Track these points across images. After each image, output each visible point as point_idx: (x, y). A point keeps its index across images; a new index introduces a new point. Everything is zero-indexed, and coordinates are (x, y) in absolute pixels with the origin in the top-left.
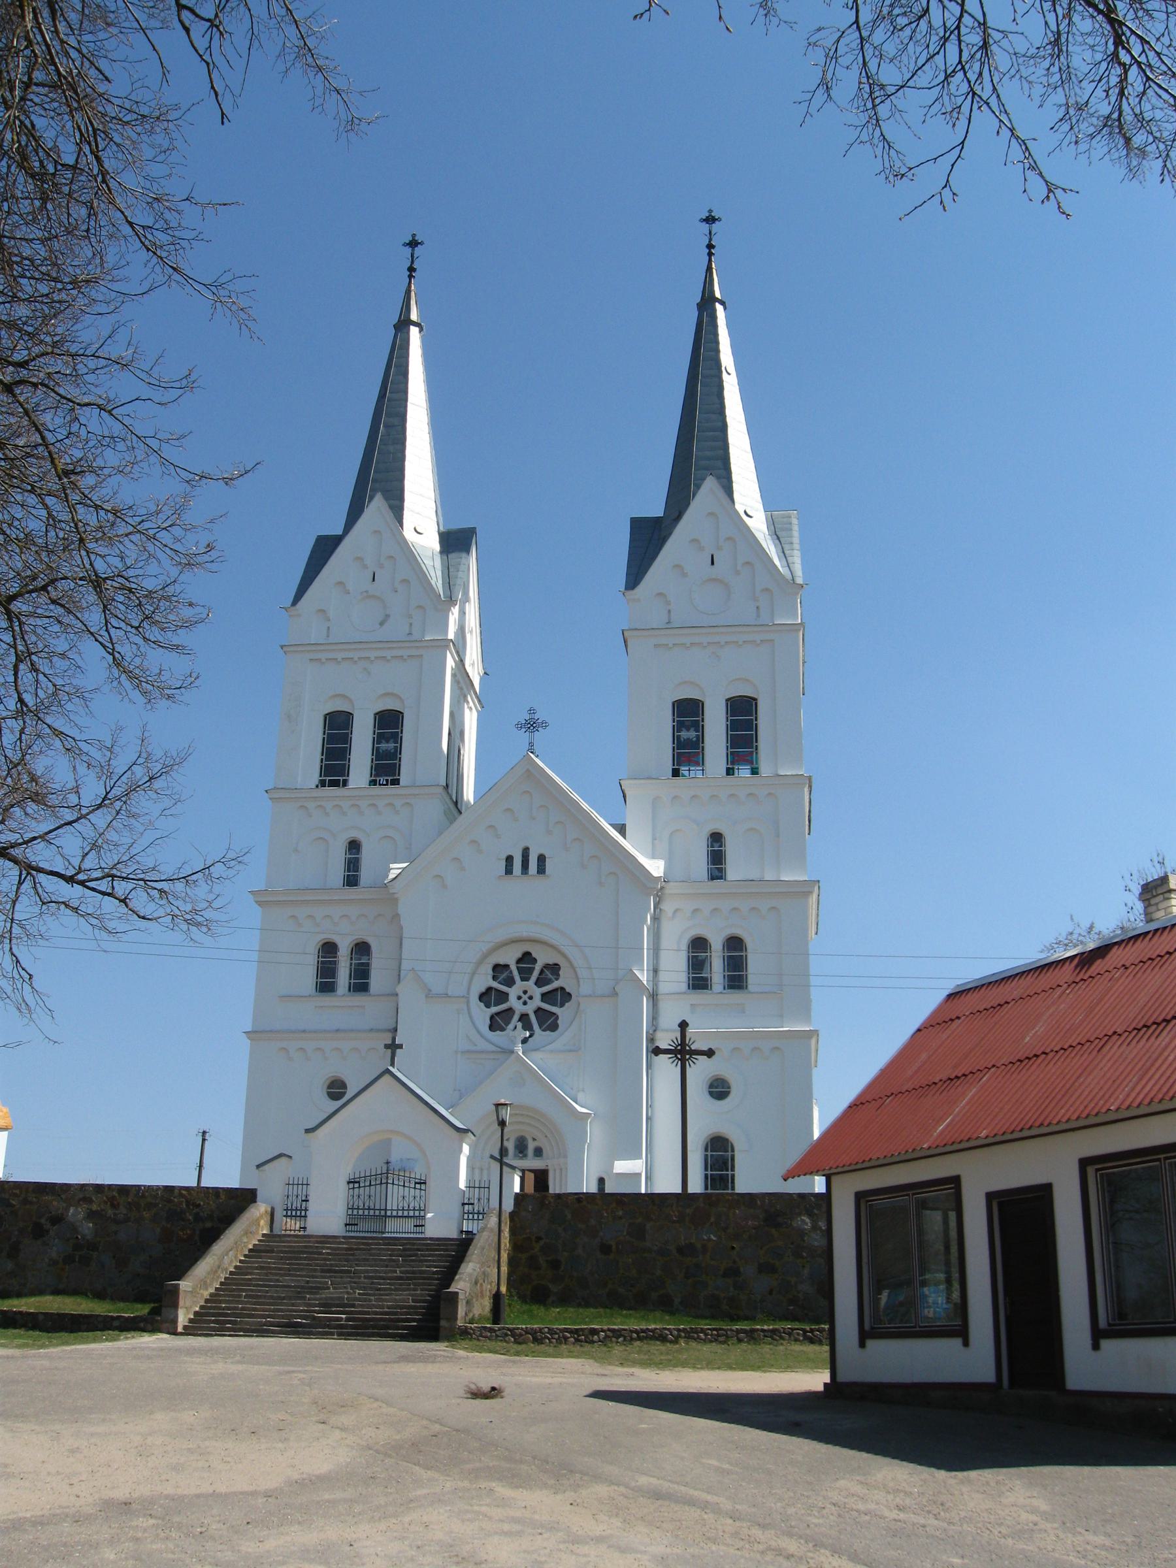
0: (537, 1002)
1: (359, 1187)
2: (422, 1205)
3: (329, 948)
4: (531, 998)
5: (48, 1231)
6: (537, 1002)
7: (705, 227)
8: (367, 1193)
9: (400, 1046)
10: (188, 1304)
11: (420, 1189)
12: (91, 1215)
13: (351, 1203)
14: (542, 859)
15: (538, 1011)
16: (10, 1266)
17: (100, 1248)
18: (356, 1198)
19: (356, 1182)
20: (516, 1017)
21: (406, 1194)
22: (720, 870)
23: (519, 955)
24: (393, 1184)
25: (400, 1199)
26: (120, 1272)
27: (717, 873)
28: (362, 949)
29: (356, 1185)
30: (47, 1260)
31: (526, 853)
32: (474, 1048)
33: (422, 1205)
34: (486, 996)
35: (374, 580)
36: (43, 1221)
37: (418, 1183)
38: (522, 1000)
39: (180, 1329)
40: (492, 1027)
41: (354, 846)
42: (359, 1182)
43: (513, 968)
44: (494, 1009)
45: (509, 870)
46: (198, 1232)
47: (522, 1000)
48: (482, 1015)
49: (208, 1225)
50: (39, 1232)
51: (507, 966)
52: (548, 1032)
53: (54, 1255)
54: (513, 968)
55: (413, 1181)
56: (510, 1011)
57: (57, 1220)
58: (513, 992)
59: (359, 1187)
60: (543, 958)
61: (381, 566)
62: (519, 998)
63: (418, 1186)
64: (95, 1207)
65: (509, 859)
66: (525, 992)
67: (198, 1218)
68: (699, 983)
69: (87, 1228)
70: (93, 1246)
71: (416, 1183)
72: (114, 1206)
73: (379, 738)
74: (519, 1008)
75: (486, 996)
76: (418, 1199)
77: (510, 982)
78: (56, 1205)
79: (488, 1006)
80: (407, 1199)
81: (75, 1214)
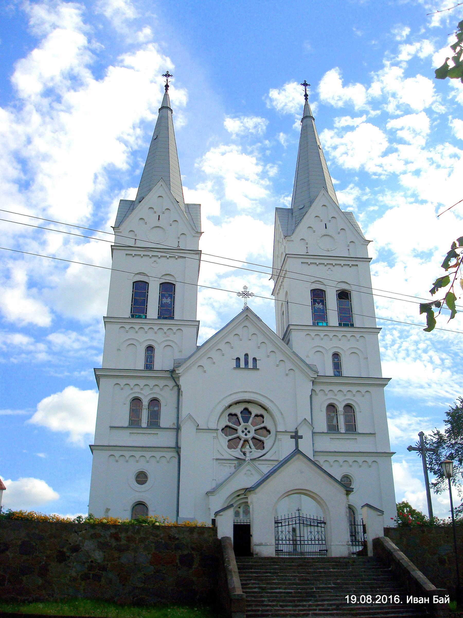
1: (282, 526)
2: (323, 537)
3: (136, 401)
4: (249, 432)
5: (68, 557)
6: (252, 434)
8: (287, 529)
9: (301, 437)
11: (321, 527)
12: (102, 546)
13: (277, 537)
14: (255, 360)
15: (254, 438)
16: (40, 581)
17: (108, 569)
18: (280, 533)
19: (279, 523)
21: (312, 530)
22: (339, 372)
23: (242, 409)
24: (303, 524)
25: (309, 533)
26: (123, 585)
27: (337, 373)
28: (155, 402)
29: (280, 525)
30: (68, 577)
31: (246, 355)
32: (222, 457)
33: (323, 537)
34: (227, 429)
35: (159, 219)
36: (65, 550)
37: (319, 523)
38: (244, 433)
40: (230, 447)
41: (150, 349)
42: (281, 523)
43: (239, 415)
44: (230, 437)
45: (238, 366)
46: (178, 557)
47: (244, 433)
48: (223, 440)
49: (185, 552)
51: (235, 415)
52: (259, 450)
53: (74, 574)
54: (239, 415)
55: (316, 521)
56: (239, 438)
57: (76, 549)
58: (240, 429)
59: (282, 526)
61: (163, 213)
62: (243, 432)
63: (319, 525)
65: (238, 359)
66: (246, 429)
67: (178, 547)
69: (98, 556)
70: (104, 568)
71: (318, 523)
72: (118, 539)
73: (162, 296)
75: (227, 429)
76: (320, 533)
78: (74, 538)
79: (226, 435)
80: (313, 533)
81: (88, 545)
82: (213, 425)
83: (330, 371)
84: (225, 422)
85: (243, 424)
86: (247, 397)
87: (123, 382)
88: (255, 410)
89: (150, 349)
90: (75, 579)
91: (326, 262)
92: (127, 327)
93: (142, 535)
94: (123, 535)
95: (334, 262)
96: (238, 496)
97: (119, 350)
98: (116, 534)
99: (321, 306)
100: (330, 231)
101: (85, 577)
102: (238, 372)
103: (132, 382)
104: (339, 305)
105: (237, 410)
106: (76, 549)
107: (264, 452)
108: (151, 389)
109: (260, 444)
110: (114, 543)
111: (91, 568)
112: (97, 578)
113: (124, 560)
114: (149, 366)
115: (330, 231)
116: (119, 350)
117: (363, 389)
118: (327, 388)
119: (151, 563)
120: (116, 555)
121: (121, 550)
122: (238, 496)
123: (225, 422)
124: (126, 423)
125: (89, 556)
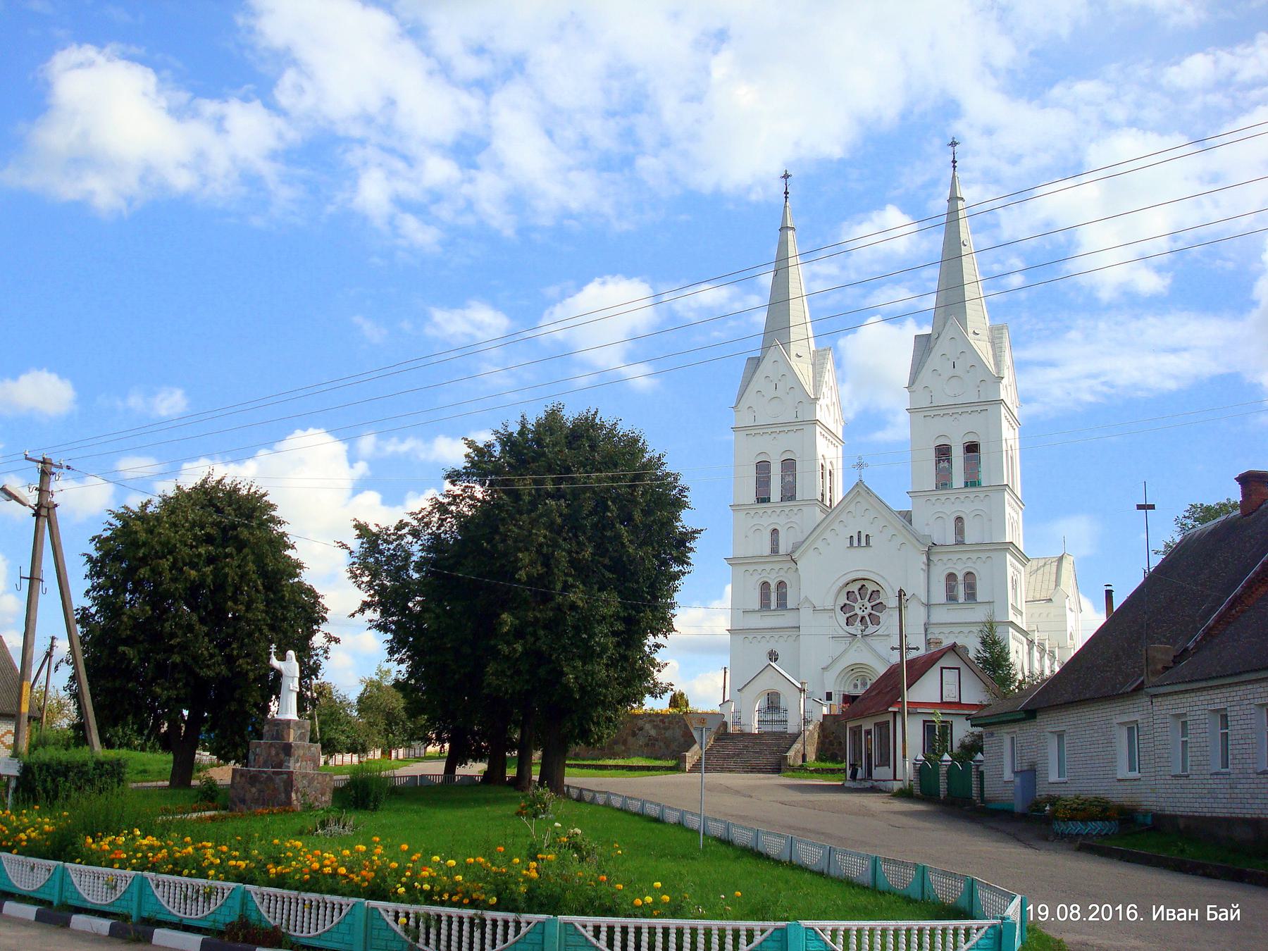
0: (869, 610)
3: (765, 585)
4: (866, 608)
6: (869, 610)
7: (951, 148)
10: (690, 761)
12: (655, 727)
20: (859, 619)
28: (781, 584)
39: (687, 770)
41: (775, 531)
48: (842, 618)
50: (634, 735)
54: (857, 593)
57: (641, 729)
58: (857, 606)
60: (871, 587)
61: (780, 380)
62: (861, 608)
64: (655, 723)
66: (863, 606)
68: (952, 598)
69: (653, 733)
74: (860, 613)
77: (855, 601)
78: (640, 723)
81: (648, 726)
82: (829, 605)
83: (951, 539)
84: (843, 600)
85: (860, 600)
86: (860, 575)
87: (751, 568)
88: (871, 587)
89: (775, 531)
90: (642, 746)
91: (950, 412)
92: (752, 512)
93: (677, 720)
94: (666, 720)
95: (960, 411)
96: (852, 670)
97: (746, 536)
98: (663, 720)
99: (946, 464)
100: (958, 371)
101: (647, 745)
102: (852, 550)
103: (759, 568)
104: (966, 460)
105: (855, 588)
106: (641, 729)
107: (878, 627)
108: (777, 573)
109: (875, 620)
110: (662, 725)
111: (650, 740)
112: (653, 745)
113: (667, 735)
114: (775, 550)
115: (958, 371)
116: (746, 536)
117: (983, 556)
118: (945, 558)
119: (683, 736)
120: (663, 732)
121: (666, 729)
122: (852, 670)
123: (843, 600)
124: (757, 606)
125: (648, 733)
